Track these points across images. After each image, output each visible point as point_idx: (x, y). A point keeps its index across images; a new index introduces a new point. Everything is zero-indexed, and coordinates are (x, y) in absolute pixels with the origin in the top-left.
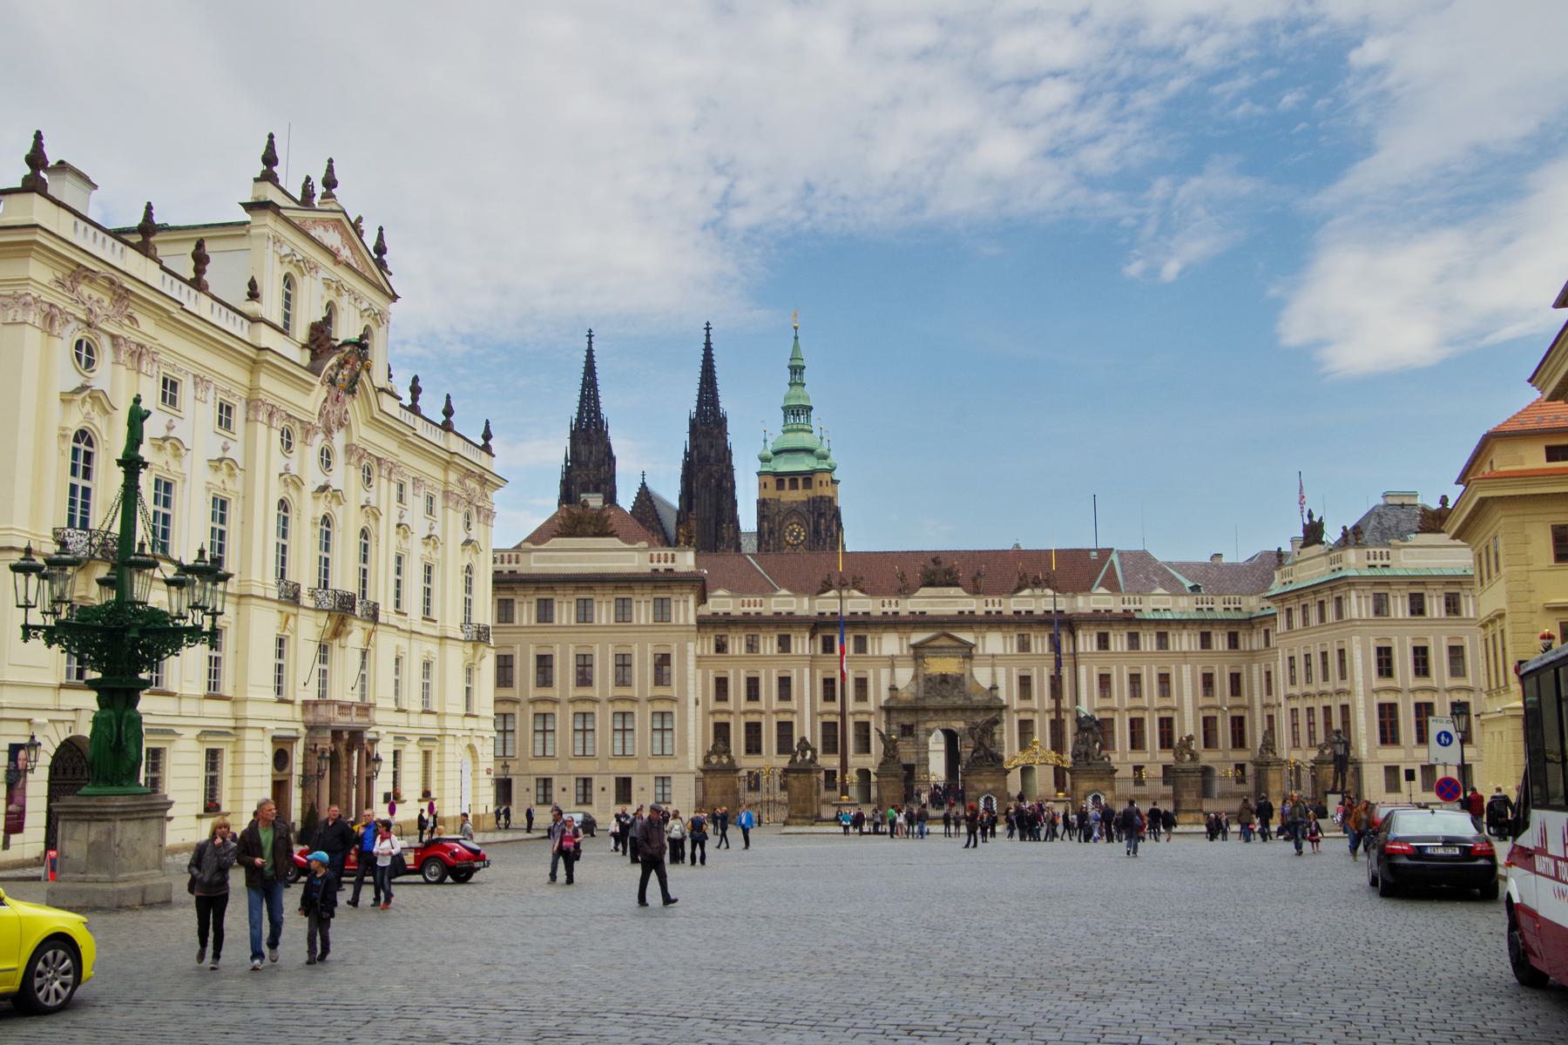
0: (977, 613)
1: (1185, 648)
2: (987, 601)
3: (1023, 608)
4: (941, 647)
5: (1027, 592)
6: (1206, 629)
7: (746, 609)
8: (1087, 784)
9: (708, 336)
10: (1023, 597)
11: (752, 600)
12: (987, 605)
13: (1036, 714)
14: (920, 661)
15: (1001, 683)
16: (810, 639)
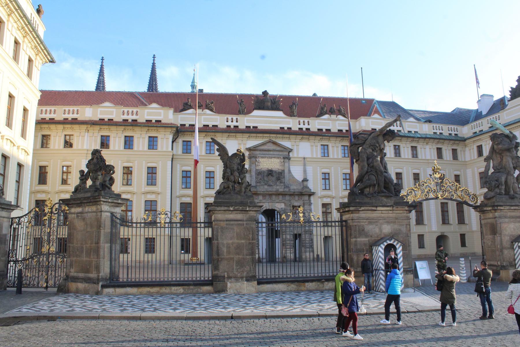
0: (293, 129)
1: (428, 157)
2: (299, 121)
3: (324, 128)
4: (269, 150)
5: (326, 116)
6: (439, 146)
7: (125, 117)
8: (512, 226)
9: (154, 60)
10: (325, 119)
11: (130, 110)
12: (299, 124)
13: (334, 200)
14: (253, 159)
15: (310, 177)
16: (173, 142)
